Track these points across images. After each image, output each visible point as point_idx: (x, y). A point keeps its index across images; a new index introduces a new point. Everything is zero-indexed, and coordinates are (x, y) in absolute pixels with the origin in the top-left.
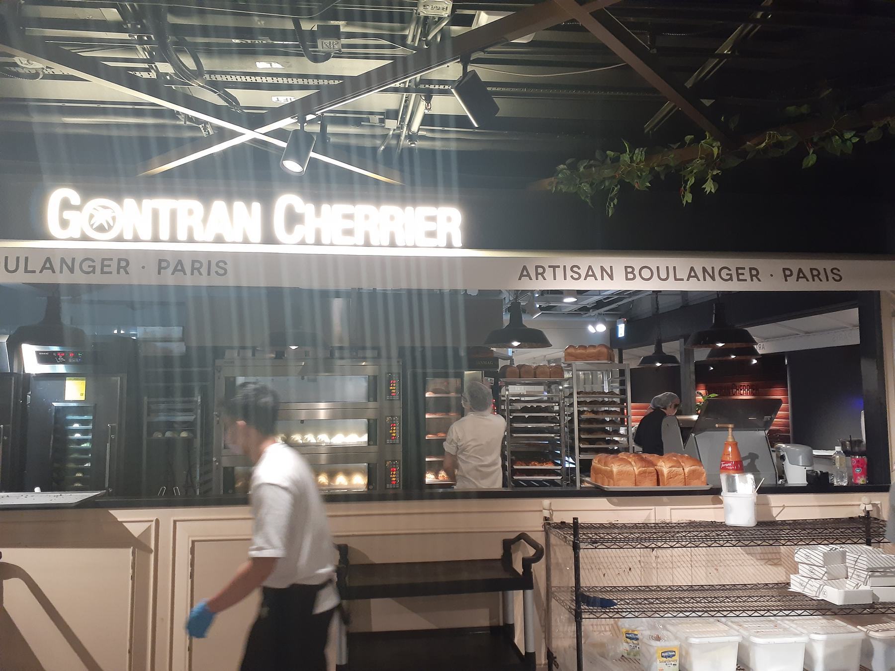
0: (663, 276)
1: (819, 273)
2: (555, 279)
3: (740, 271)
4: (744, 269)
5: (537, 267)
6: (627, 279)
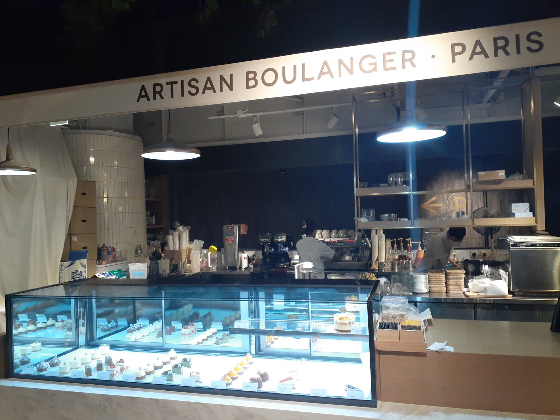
2: (172, 96)
3: (388, 57)
4: (394, 53)
5: (155, 85)
6: (248, 87)
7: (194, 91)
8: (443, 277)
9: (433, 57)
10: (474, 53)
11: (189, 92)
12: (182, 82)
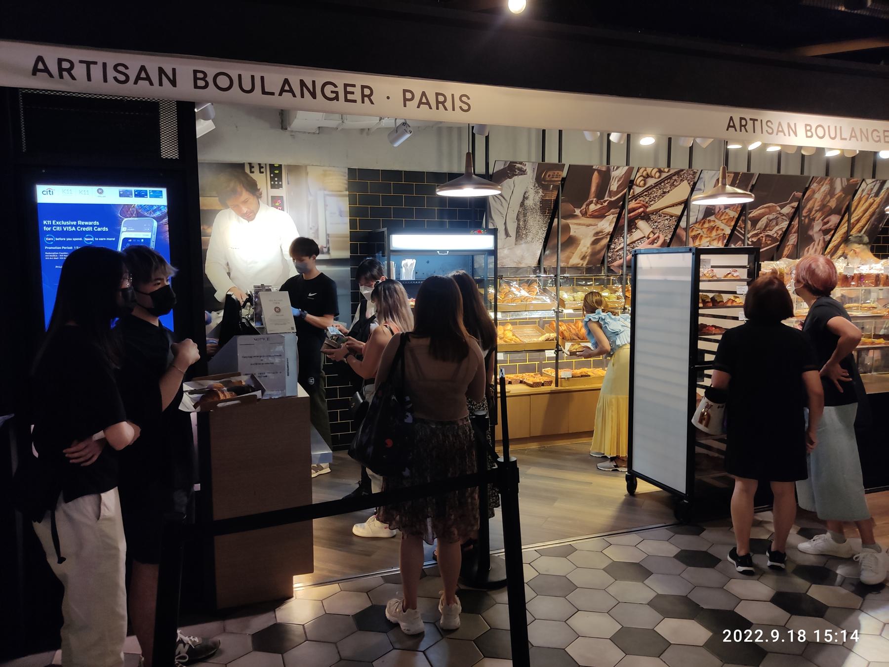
0: (833, 135)
1: (445, 100)
3: (349, 89)
4: (354, 86)
6: (196, 87)
7: (122, 78)
8: (346, 254)
9: (388, 98)
10: (420, 103)
11: (115, 78)
12: (105, 65)
